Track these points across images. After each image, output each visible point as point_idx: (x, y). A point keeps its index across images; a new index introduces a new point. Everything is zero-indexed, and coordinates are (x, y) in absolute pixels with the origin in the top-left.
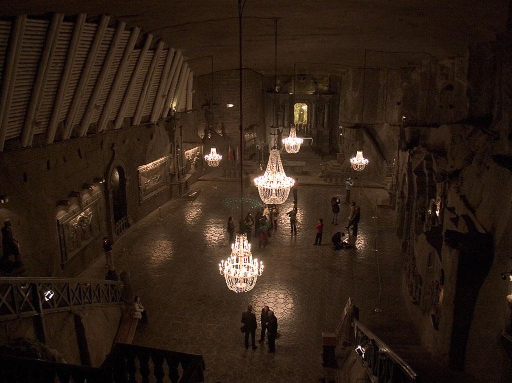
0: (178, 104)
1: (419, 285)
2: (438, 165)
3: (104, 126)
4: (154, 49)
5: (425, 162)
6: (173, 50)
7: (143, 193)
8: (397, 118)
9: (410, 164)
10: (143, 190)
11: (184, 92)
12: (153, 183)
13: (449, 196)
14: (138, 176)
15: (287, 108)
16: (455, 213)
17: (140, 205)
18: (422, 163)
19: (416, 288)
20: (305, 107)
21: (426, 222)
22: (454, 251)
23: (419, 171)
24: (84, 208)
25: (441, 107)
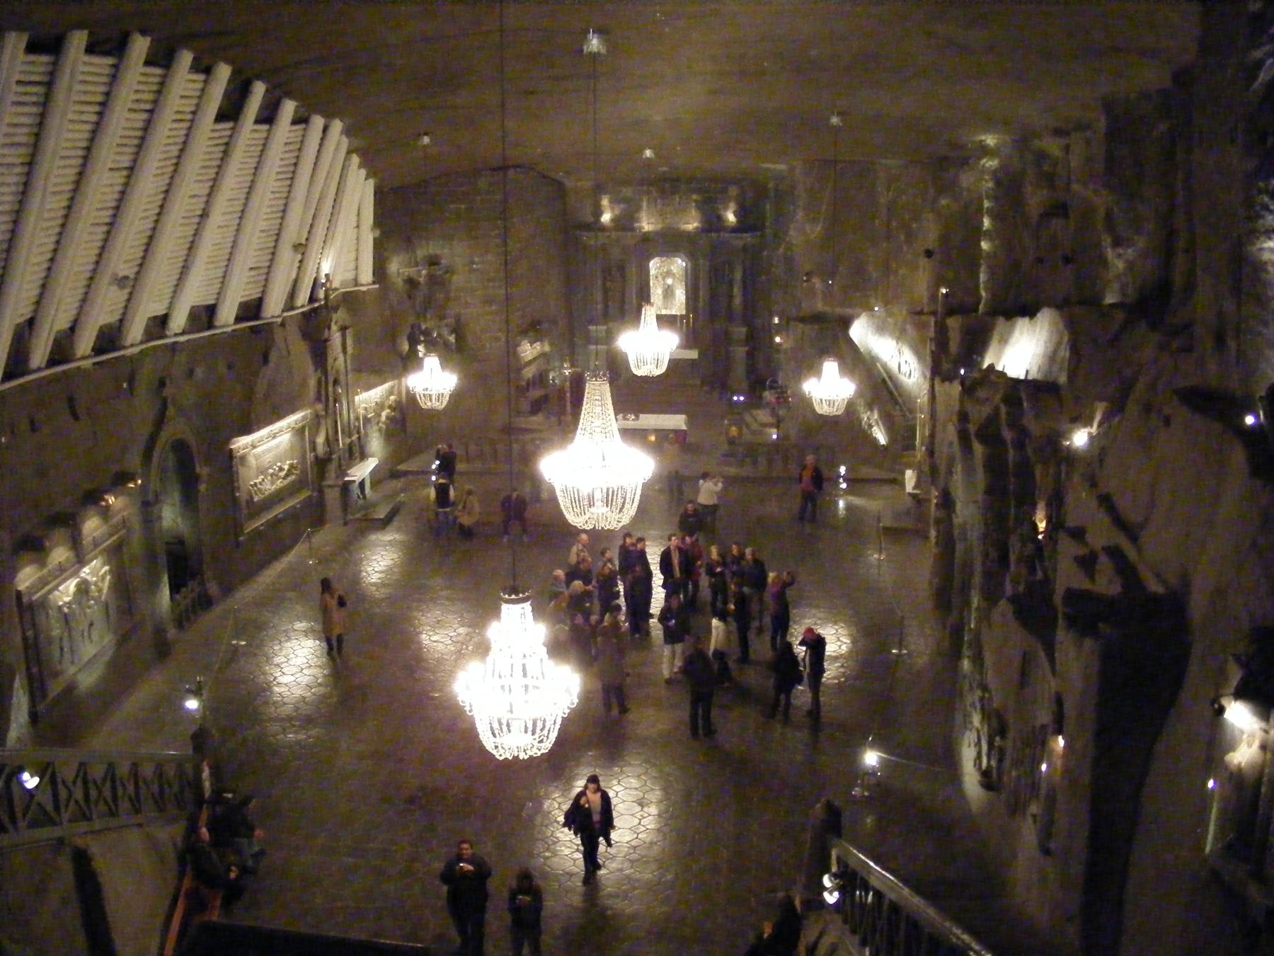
0: (336, 267)
1: (998, 738)
2: (1037, 416)
3: (135, 332)
4: (268, 116)
6: (318, 122)
7: (246, 511)
8: (925, 294)
9: (963, 417)
10: (244, 504)
11: (352, 233)
12: (272, 483)
13: (1070, 499)
14: (231, 467)
15: (632, 271)
16: (1086, 544)
17: (238, 544)
18: (997, 409)
19: (991, 744)
20: (679, 264)
21: (1013, 568)
22: (1088, 643)
23: (989, 434)
24: (88, 557)
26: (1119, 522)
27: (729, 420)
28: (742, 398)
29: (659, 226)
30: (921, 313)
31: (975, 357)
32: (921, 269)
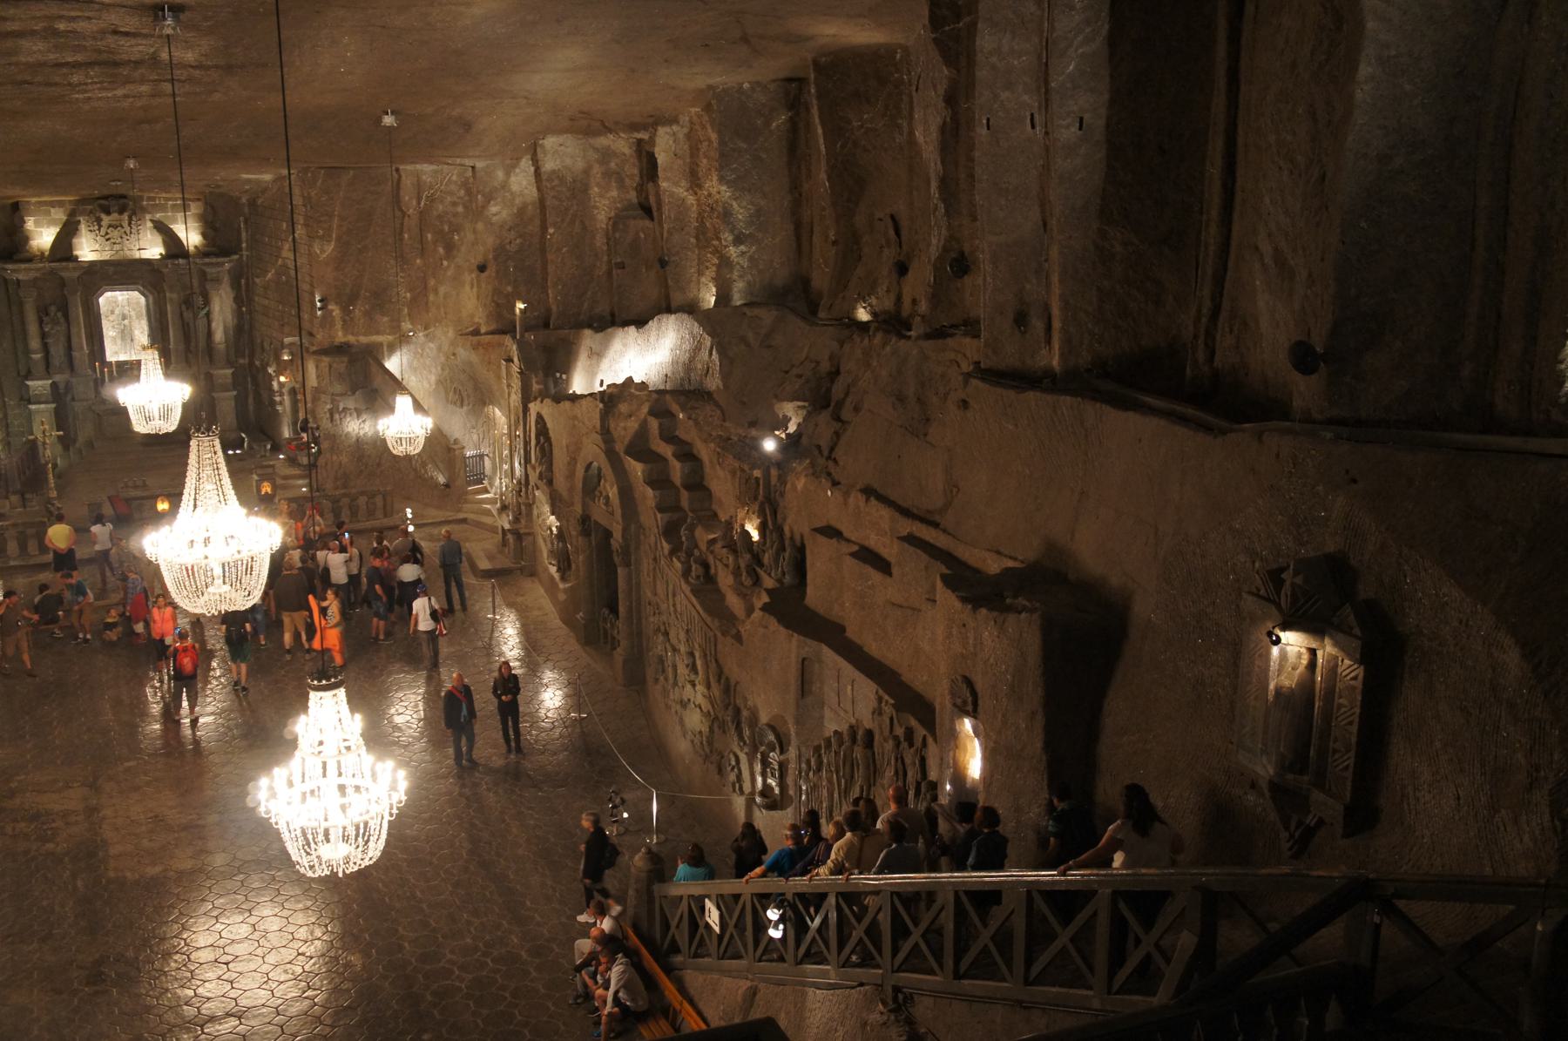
2: (697, 423)
5: (654, 424)
9: (606, 432)
16: (848, 541)
19: (765, 763)
21: (725, 580)
23: (640, 449)
25: (622, 266)
26: (906, 512)
27: (258, 475)
28: (238, 452)
29: (106, 256)
30: (476, 333)
31: (558, 375)
32: (467, 288)
